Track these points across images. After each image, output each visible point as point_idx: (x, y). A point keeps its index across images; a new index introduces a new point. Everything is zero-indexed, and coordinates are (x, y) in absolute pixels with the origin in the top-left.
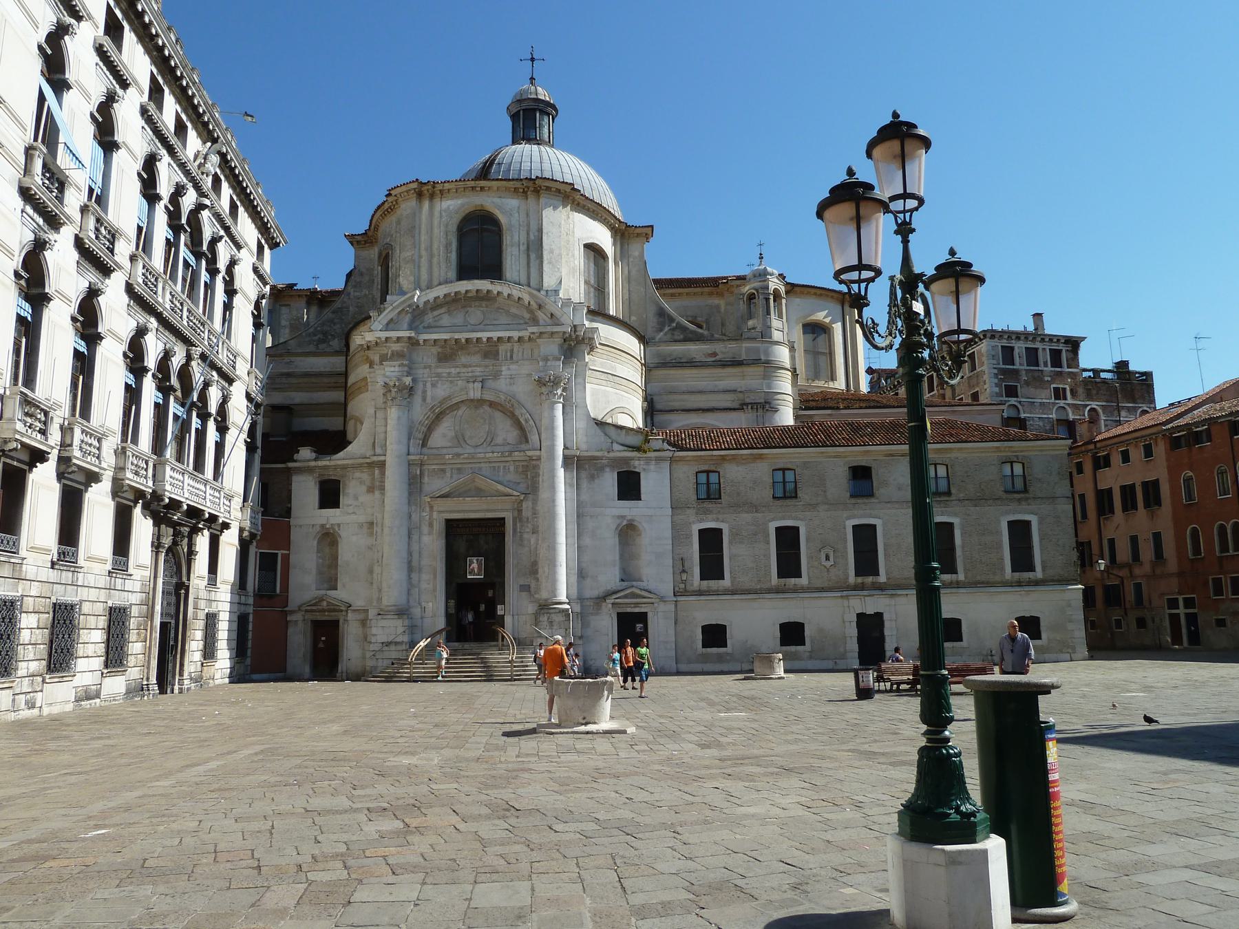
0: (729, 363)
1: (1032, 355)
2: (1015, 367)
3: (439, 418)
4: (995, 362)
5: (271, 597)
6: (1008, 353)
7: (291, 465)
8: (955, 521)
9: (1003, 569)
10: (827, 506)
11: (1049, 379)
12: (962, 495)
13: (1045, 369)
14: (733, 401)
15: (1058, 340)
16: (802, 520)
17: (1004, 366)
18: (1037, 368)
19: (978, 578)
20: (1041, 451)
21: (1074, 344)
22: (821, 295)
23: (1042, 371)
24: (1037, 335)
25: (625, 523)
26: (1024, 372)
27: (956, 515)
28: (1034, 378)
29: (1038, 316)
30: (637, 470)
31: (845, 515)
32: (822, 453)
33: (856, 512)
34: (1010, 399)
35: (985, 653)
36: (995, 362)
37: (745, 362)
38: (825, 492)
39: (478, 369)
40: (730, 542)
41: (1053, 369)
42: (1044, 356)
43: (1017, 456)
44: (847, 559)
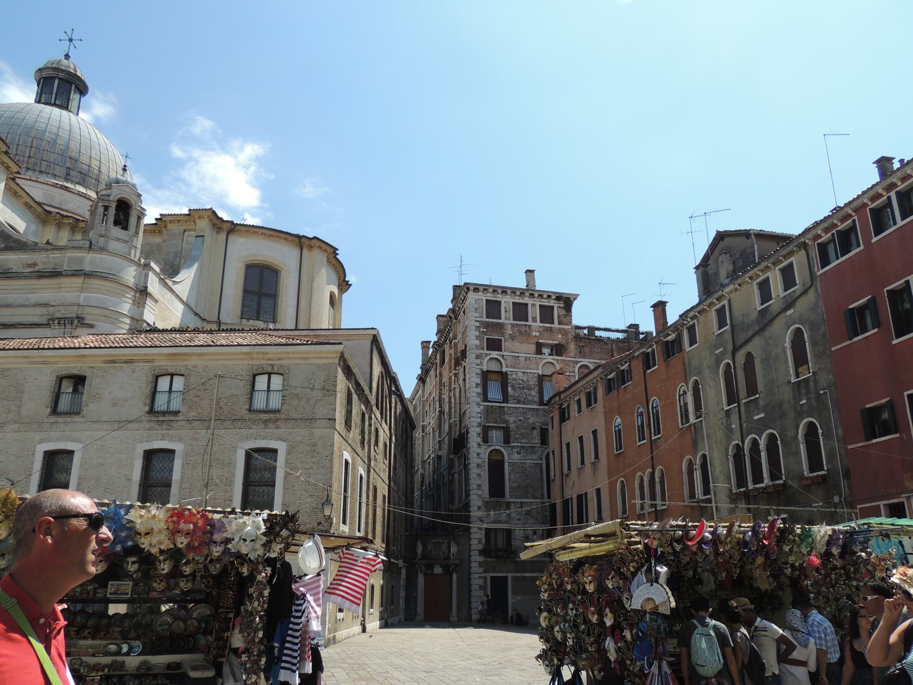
0: (47, 274)
1: (520, 311)
2: (500, 321)
4: (477, 315)
6: (493, 308)
8: (178, 447)
10: (16, 426)
11: (538, 334)
12: (192, 414)
13: (534, 324)
14: (42, 316)
15: (549, 297)
17: (487, 320)
18: (524, 323)
20: (305, 359)
21: (567, 301)
22: (273, 236)
23: (530, 326)
24: (530, 291)
26: (510, 327)
27: (180, 439)
28: (521, 333)
29: (530, 272)
31: (37, 438)
32: (26, 357)
33: (52, 434)
34: (491, 352)
36: (477, 315)
37: (64, 273)
38: (19, 407)
41: (542, 325)
42: (534, 312)
43: (272, 366)
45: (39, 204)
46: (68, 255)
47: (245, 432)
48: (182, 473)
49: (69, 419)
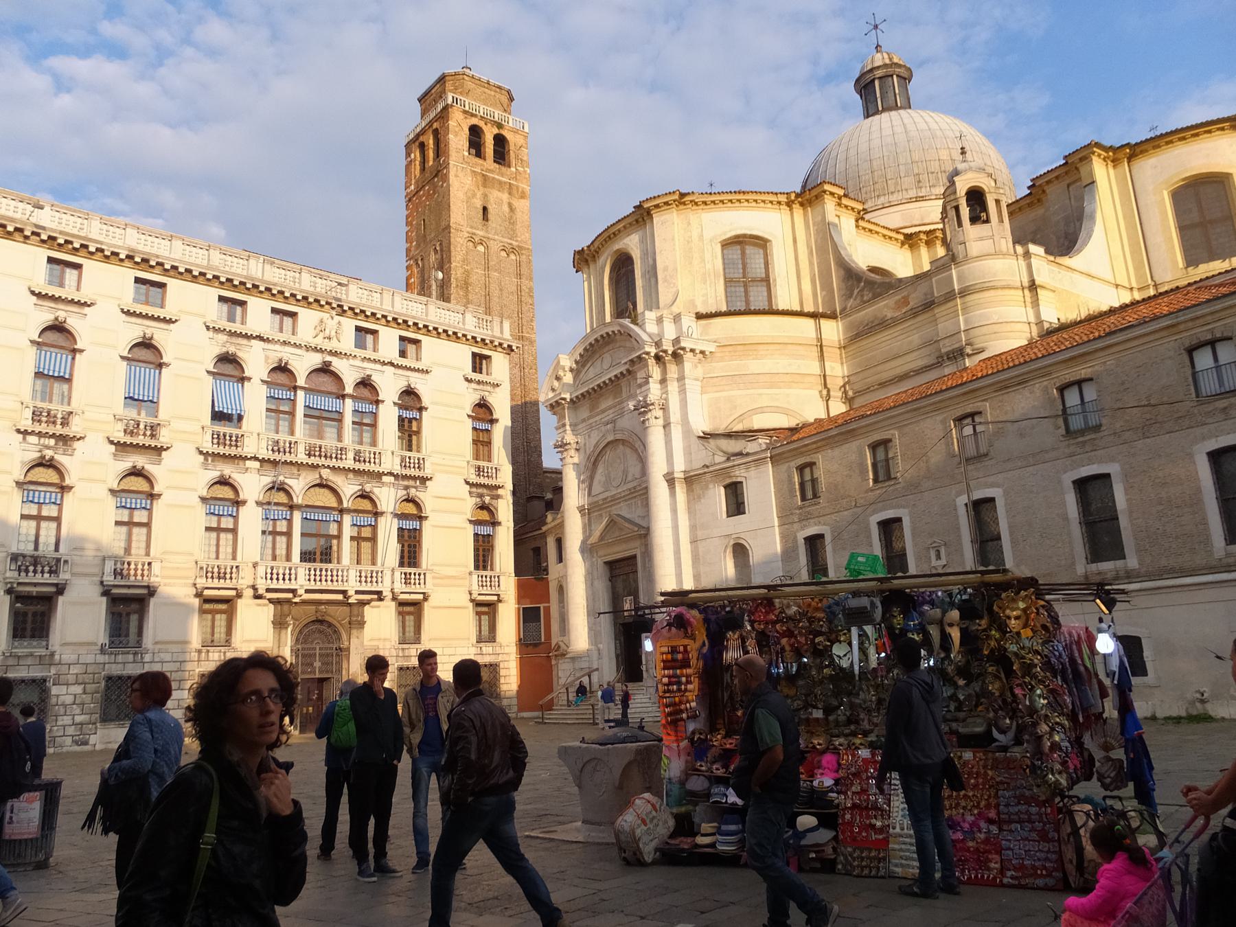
3: (595, 464)
5: (535, 645)
7: (544, 528)
8: (1112, 469)
9: (1207, 541)
12: (1118, 425)
16: (904, 507)
19: (1164, 562)
25: (732, 542)
27: (1112, 459)
30: (739, 480)
32: (915, 410)
35: (1189, 696)
39: (611, 411)
40: (834, 550)
43: (1212, 331)
44: (962, 555)
45: (897, 231)
46: (934, 280)
47: (1198, 431)
48: (1127, 500)
49: (979, 465)
